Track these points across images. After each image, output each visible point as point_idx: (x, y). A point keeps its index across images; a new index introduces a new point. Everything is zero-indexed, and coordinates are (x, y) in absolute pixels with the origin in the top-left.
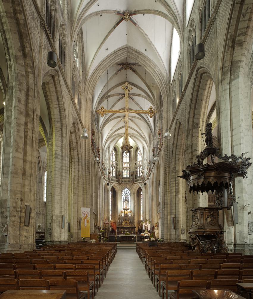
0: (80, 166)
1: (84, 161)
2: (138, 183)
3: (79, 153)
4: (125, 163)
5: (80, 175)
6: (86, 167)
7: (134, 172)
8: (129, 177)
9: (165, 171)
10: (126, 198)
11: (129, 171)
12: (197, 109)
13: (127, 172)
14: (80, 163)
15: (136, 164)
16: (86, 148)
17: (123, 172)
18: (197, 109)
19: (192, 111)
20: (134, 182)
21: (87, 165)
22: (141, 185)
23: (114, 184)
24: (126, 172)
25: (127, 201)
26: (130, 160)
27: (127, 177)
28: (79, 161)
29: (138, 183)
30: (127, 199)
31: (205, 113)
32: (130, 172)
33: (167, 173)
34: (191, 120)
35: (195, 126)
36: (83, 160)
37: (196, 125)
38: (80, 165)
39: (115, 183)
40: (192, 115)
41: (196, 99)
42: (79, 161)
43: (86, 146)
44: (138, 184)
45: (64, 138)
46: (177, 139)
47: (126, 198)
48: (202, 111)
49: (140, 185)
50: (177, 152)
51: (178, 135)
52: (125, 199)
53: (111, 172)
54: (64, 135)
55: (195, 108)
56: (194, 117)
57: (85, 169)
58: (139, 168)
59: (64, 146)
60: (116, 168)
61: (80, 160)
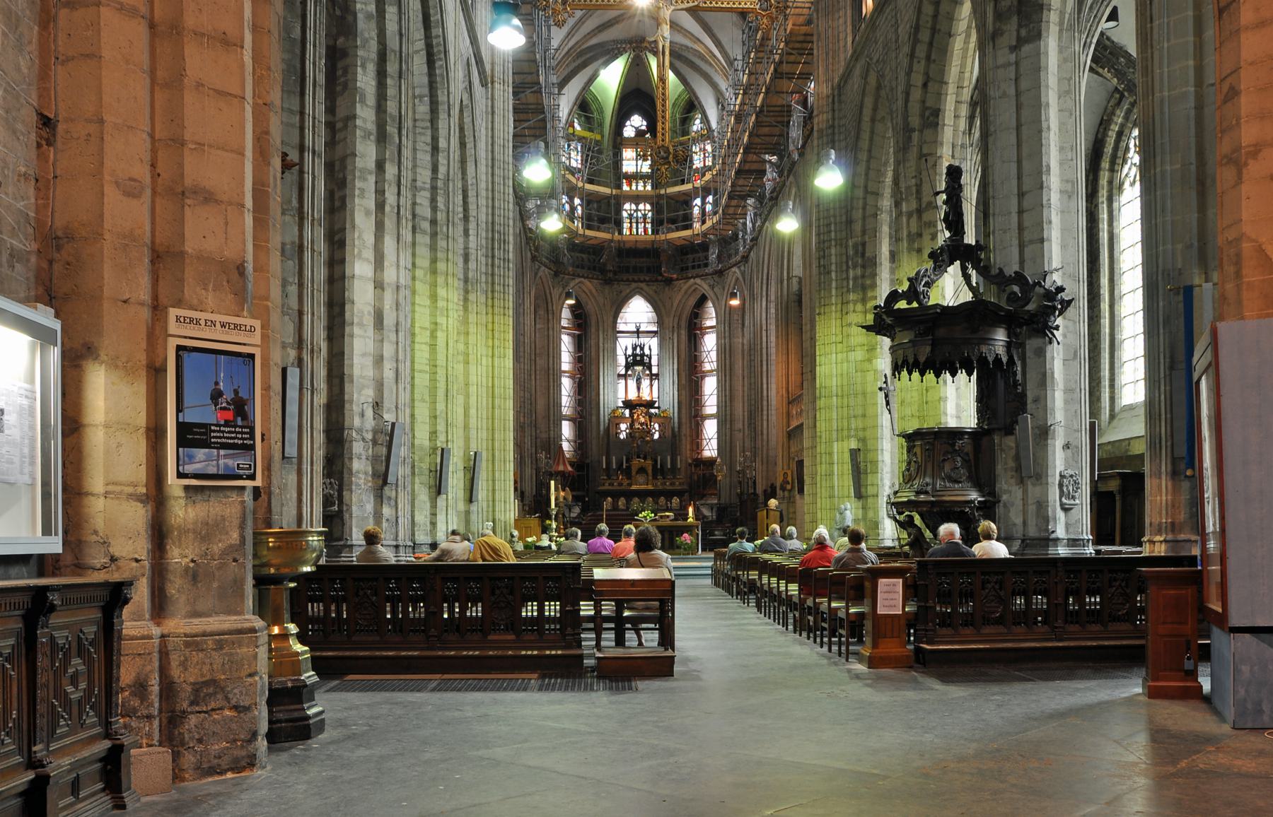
0: (471, 238)
1: (487, 214)
2: (698, 276)
3: (470, 182)
5: (470, 275)
6: (493, 239)
9: (824, 257)
10: (638, 351)
12: (934, 61)
14: (472, 226)
16: (493, 159)
18: (934, 61)
19: (919, 67)
21: (499, 232)
25: (641, 363)
28: (466, 218)
30: (643, 355)
31: (967, 75)
33: (833, 267)
34: (916, 94)
35: (928, 118)
36: (484, 209)
37: (932, 114)
38: (471, 232)
40: (918, 79)
41: (934, 31)
42: (466, 218)
43: (493, 152)
44: (698, 281)
45: (440, 154)
46: (872, 132)
47: (638, 351)
48: (953, 69)
49: (706, 287)
50: (870, 184)
51: (873, 120)
52: (634, 355)
54: (442, 143)
55: (928, 58)
56: (925, 85)
57: (493, 249)
58: (698, 201)
59: (440, 184)
61: (472, 212)
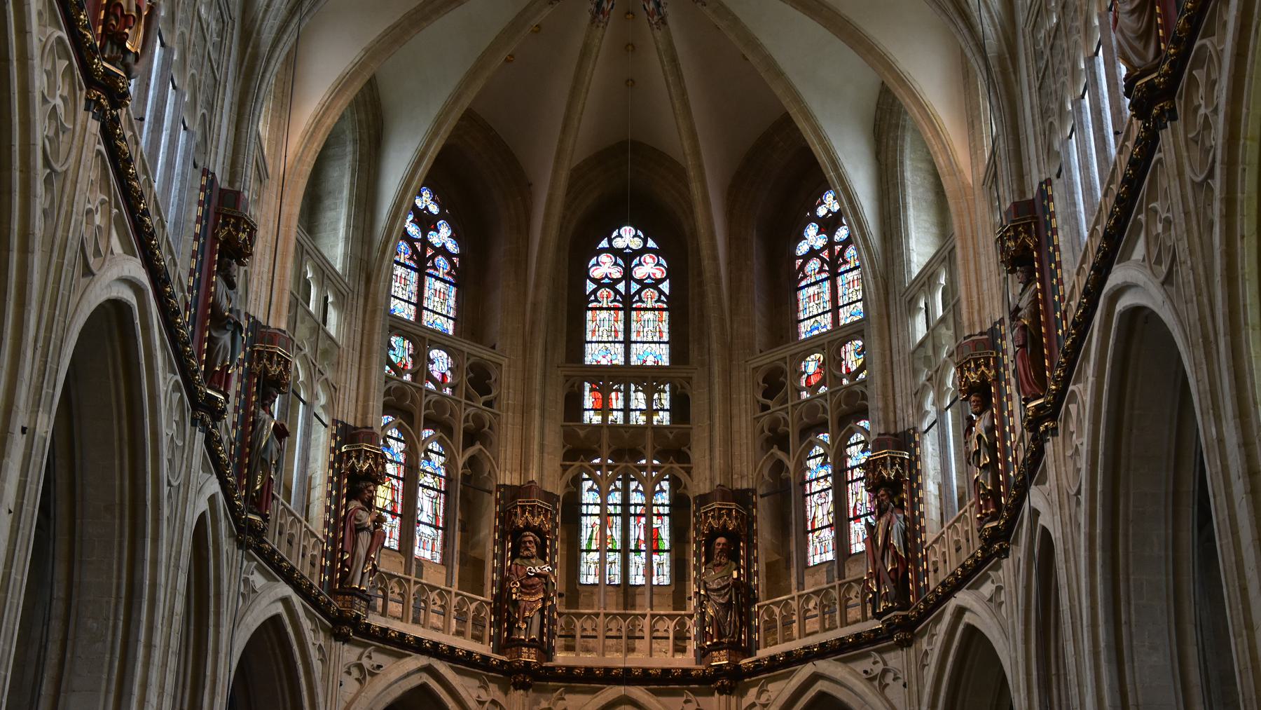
2: (824, 651)
4: (607, 378)
7: (743, 498)
8: (663, 577)
11: (664, 498)
13: (636, 498)
15: (768, 394)
17: (572, 511)
20: (749, 652)
22: (878, 681)
23: (415, 662)
24: (616, 498)
26: (679, 342)
27: (637, 579)
29: (824, 651)
32: (679, 505)
39: (435, 650)
44: (823, 666)
53: (377, 477)
60: (471, 437)
